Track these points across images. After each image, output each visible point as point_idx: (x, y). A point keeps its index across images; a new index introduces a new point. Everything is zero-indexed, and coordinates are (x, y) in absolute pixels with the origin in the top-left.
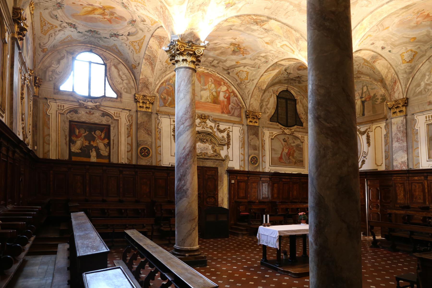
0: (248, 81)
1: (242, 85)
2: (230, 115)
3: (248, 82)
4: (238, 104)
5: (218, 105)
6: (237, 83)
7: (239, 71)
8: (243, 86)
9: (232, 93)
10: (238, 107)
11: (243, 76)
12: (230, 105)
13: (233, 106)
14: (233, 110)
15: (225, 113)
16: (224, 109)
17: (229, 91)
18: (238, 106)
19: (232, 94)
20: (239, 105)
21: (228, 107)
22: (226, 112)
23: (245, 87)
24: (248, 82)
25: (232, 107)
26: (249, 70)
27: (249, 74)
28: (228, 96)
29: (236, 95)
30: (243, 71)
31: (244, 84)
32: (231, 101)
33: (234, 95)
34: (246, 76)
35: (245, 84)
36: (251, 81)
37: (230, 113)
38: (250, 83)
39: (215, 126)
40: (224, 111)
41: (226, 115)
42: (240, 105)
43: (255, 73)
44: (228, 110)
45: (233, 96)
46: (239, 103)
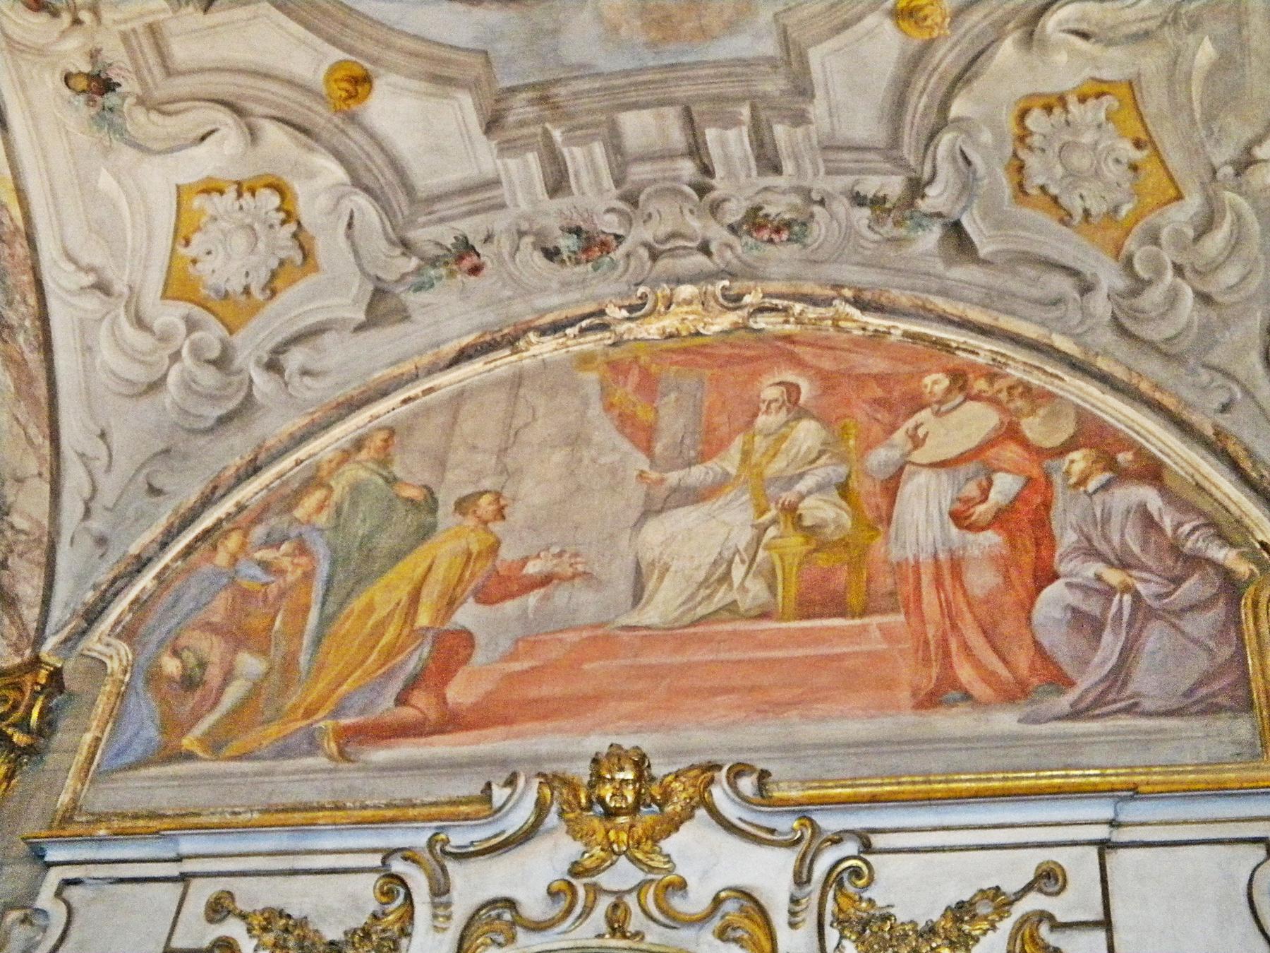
0: (1193, 202)
1: (1153, 297)
2: (1064, 702)
3: (1206, 225)
4: (1175, 549)
5: (874, 621)
6: (1100, 306)
7: (1010, 126)
8: (1173, 298)
9: (1076, 455)
10: (1193, 588)
11: (1097, 174)
12: (1053, 591)
13: (1108, 593)
14: (1111, 644)
15: (980, 689)
16: (966, 648)
17: (1025, 443)
18: (1177, 581)
19: (1078, 460)
20: (1196, 562)
21: (1027, 607)
22: (988, 677)
23: (1205, 299)
24: (1206, 225)
25: (1092, 606)
26: (1116, 53)
27: (1155, 100)
28: (1017, 498)
29: (1140, 452)
30: (1054, 103)
31: (1169, 276)
32: (1067, 538)
33: (1111, 464)
34: (1127, 150)
35: (1179, 270)
36: (1238, 190)
37: (1061, 682)
38: (1239, 217)
39: (801, 878)
40: (965, 673)
41: (1006, 721)
42: (1221, 554)
43: (1206, 53)
44: (1023, 660)
45: (1092, 485)
46: (1197, 543)
